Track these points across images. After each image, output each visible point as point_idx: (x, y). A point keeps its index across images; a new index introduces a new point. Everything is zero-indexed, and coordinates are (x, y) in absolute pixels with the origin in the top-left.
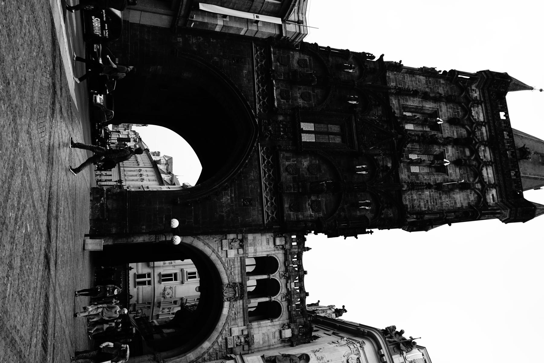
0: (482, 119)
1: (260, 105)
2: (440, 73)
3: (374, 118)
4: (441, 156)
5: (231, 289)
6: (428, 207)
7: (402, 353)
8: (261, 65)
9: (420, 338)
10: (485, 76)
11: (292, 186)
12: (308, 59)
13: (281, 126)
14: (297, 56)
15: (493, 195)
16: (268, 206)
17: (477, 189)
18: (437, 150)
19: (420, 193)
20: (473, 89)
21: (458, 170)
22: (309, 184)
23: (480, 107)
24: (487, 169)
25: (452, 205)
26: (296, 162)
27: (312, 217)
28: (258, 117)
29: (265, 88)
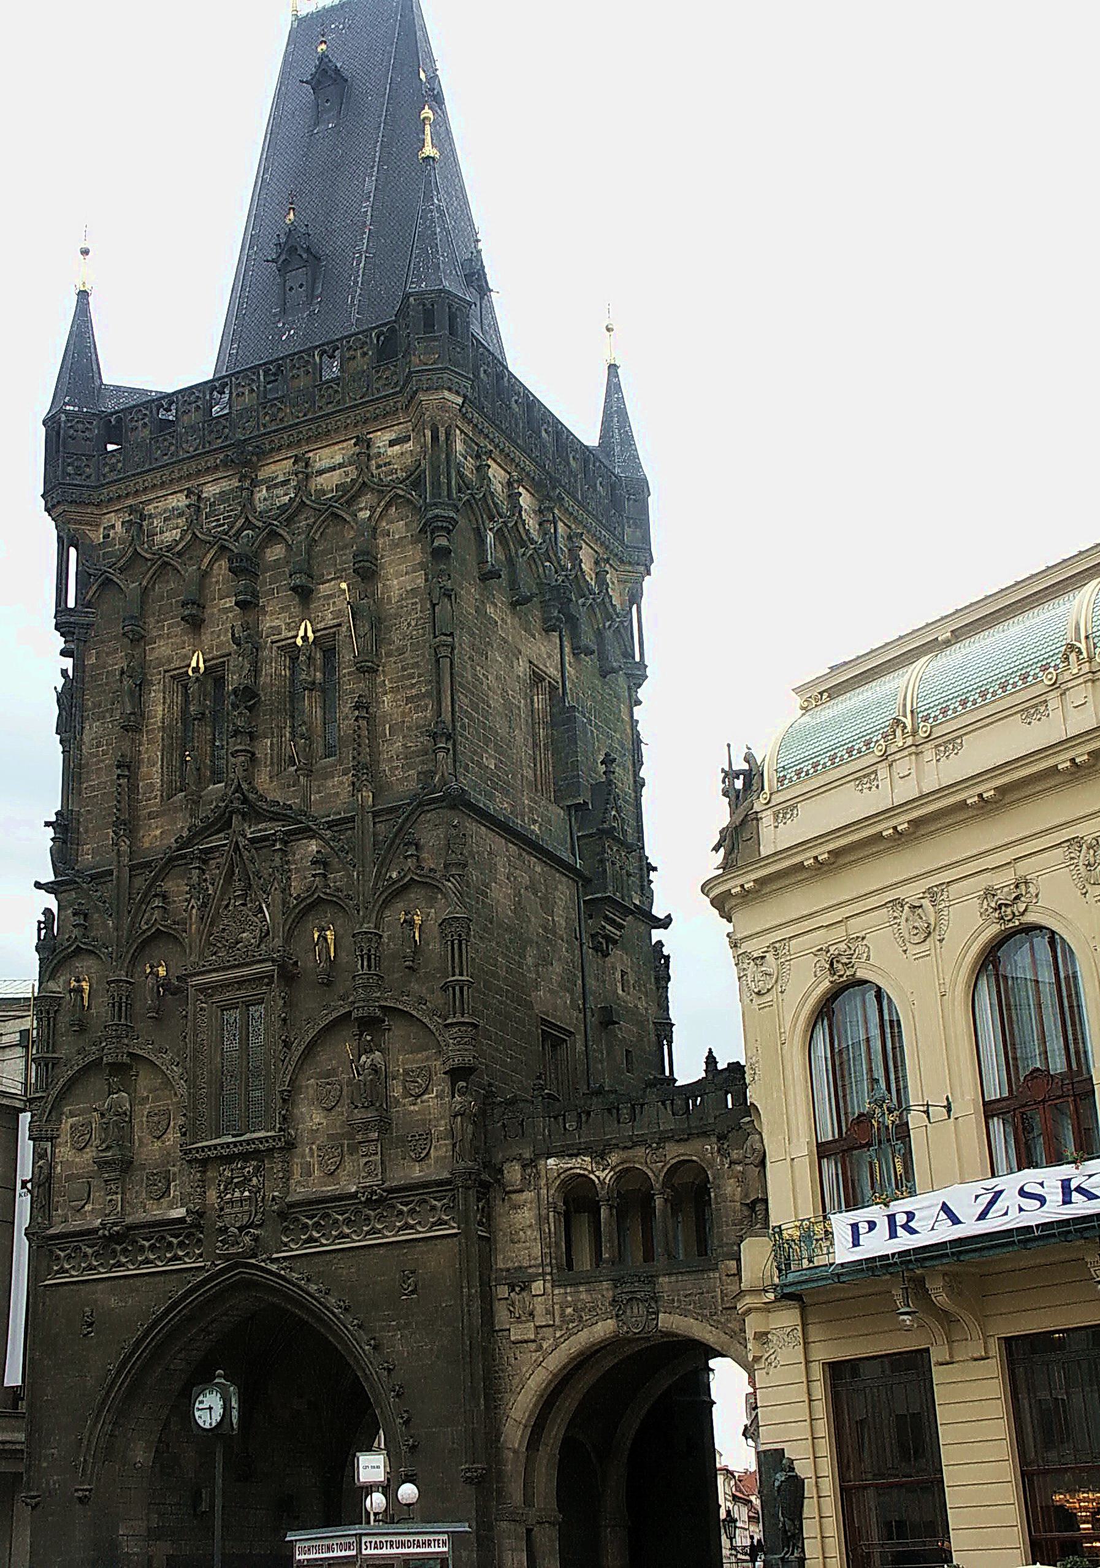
0: (179, 501)
1: (187, 1255)
2: (70, 673)
3: (194, 911)
4: (291, 651)
5: (628, 1311)
6: (424, 696)
7: (753, 816)
8: (96, 1255)
9: (729, 746)
10: (60, 509)
11: (366, 1159)
12: (71, 1120)
13: (229, 1196)
14: (65, 1152)
15: (392, 444)
16: (419, 1223)
17: (370, 517)
18: (274, 669)
19: (387, 726)
20: (104, 538)
21: (324, 589)
22: (356, 1111)
23: (150, 509)
24: (321, 473)
25: (419, 606)
26: (314, 1147)
27: (443, 1091)
28: (213, 1262)
29: (147, 1244)
